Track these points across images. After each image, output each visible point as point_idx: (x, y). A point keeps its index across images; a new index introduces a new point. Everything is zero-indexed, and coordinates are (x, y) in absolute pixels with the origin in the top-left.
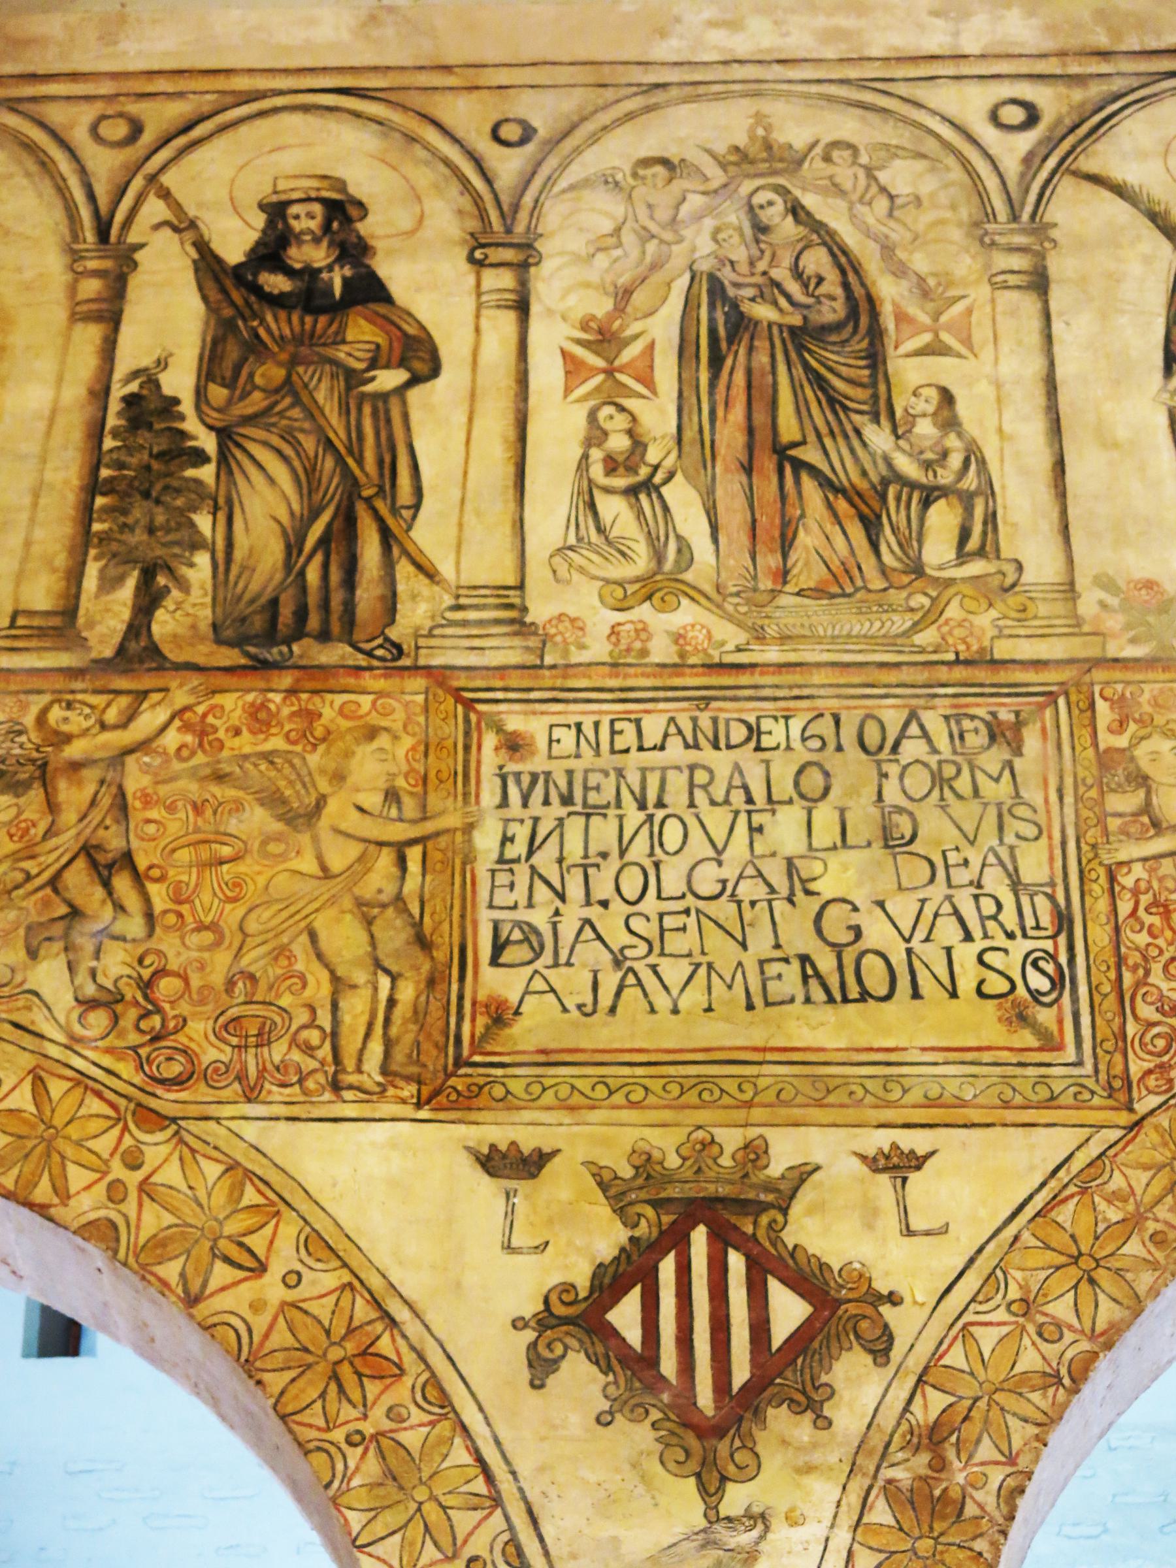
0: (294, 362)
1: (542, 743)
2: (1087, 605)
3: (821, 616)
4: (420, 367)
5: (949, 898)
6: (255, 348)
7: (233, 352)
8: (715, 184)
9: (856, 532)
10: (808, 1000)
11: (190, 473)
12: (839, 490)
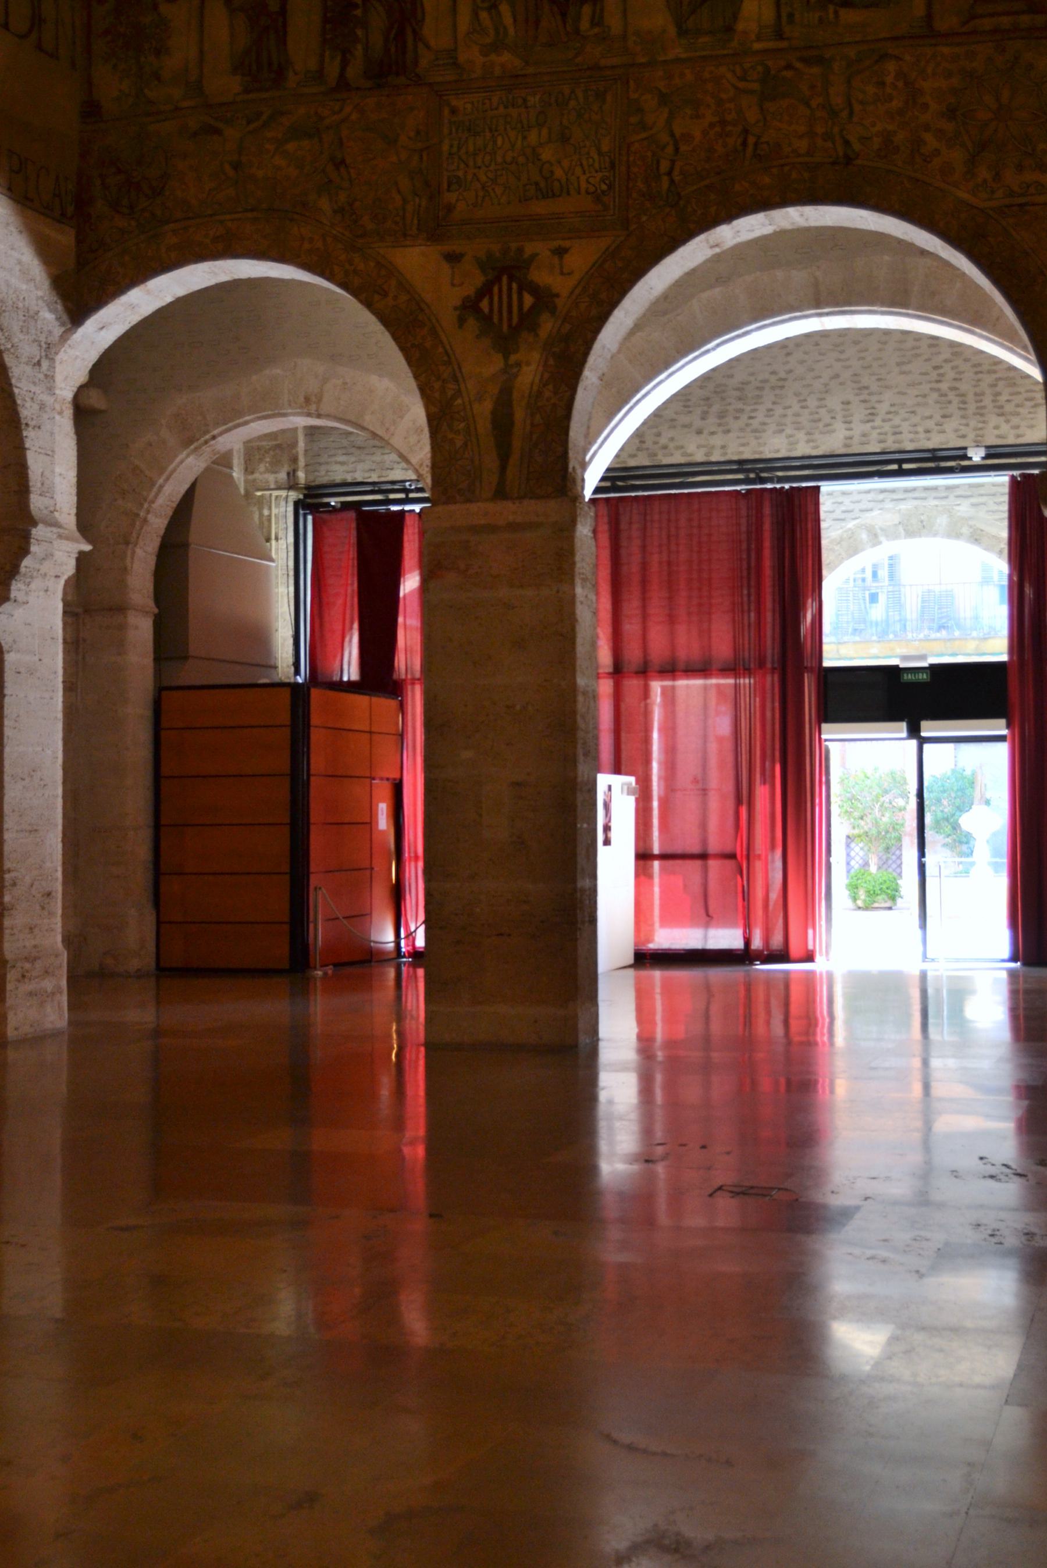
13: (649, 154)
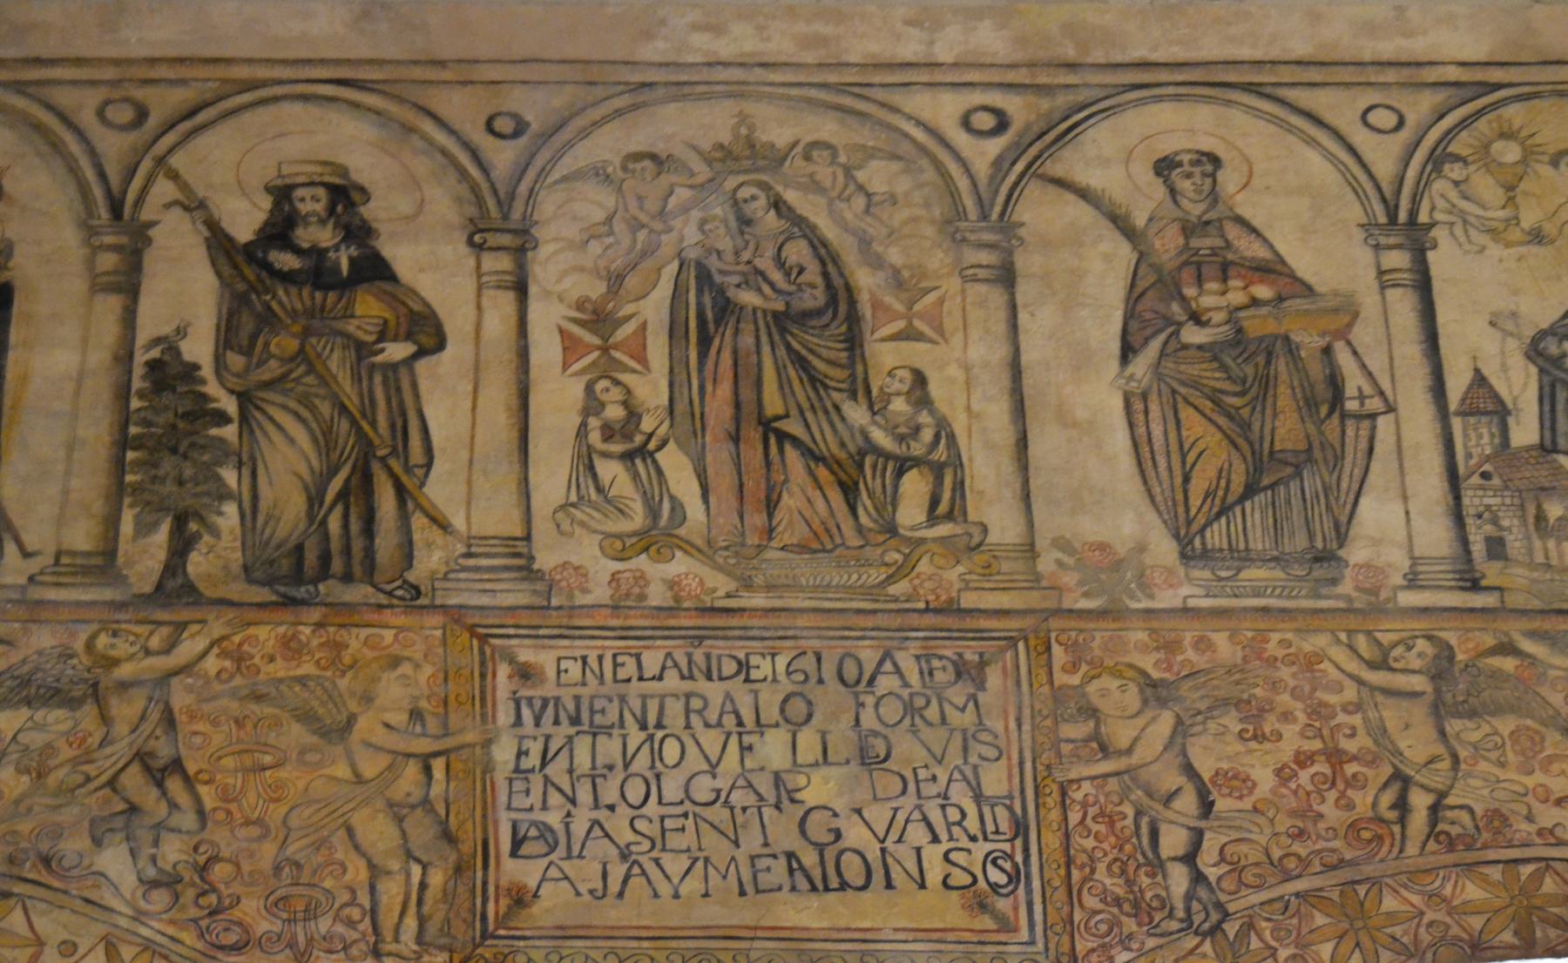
0: (306, 333)
1: (551, 673)
2: (1046, 564)
3: (807, 570)
4: (427, 341)
5: (919, 807)
6: (268, 320)
7: (247, 324)
8: (700, 179)
9: (836, 497)
10: (793, 889)
11: (214, 432)
12: (819, 459)
13: (1129, 810)
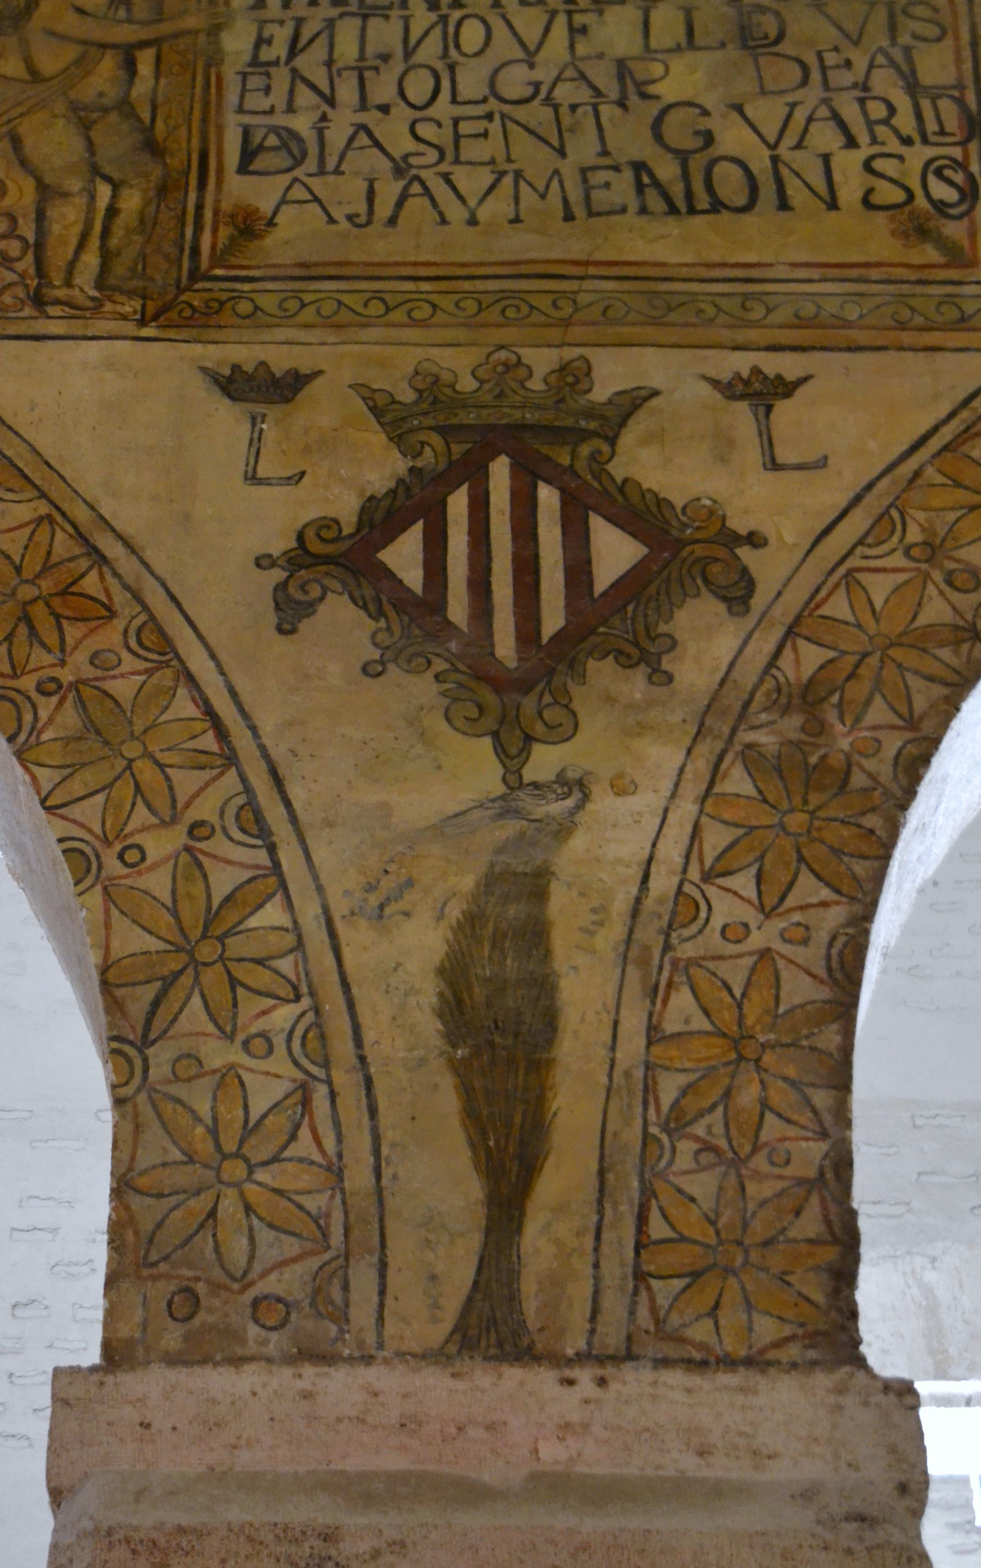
5: (826, 101)
10: (643, 210)
